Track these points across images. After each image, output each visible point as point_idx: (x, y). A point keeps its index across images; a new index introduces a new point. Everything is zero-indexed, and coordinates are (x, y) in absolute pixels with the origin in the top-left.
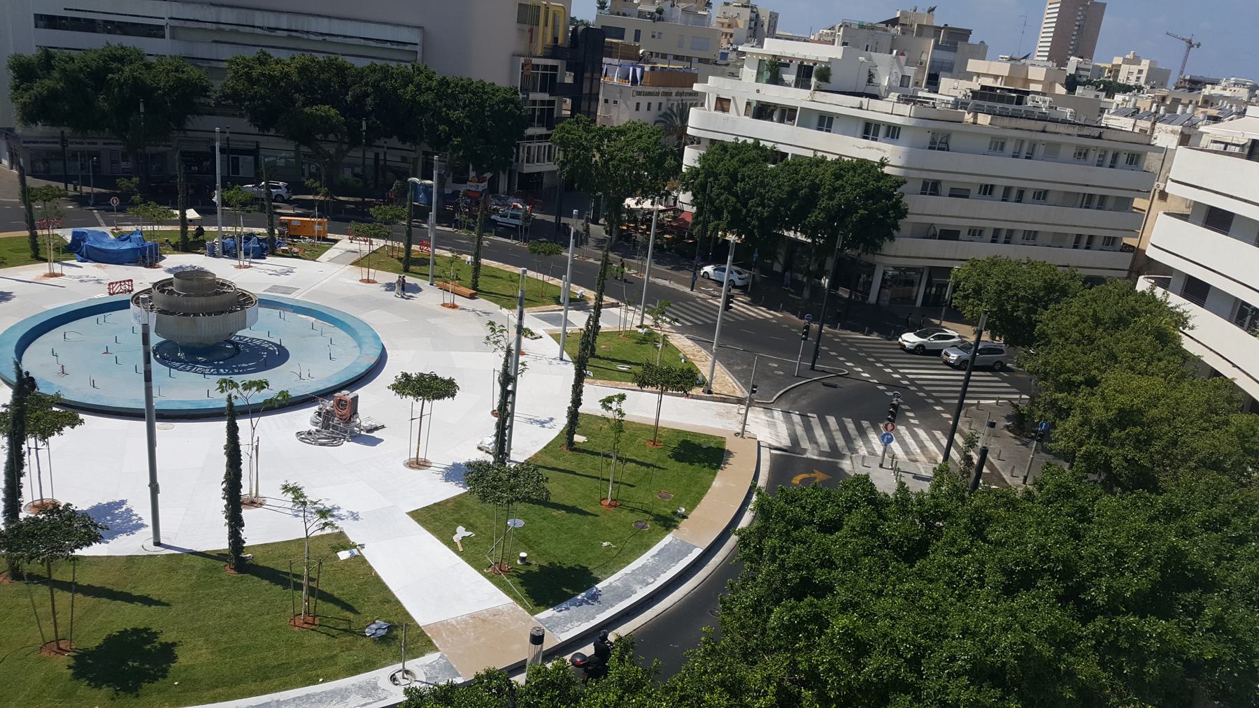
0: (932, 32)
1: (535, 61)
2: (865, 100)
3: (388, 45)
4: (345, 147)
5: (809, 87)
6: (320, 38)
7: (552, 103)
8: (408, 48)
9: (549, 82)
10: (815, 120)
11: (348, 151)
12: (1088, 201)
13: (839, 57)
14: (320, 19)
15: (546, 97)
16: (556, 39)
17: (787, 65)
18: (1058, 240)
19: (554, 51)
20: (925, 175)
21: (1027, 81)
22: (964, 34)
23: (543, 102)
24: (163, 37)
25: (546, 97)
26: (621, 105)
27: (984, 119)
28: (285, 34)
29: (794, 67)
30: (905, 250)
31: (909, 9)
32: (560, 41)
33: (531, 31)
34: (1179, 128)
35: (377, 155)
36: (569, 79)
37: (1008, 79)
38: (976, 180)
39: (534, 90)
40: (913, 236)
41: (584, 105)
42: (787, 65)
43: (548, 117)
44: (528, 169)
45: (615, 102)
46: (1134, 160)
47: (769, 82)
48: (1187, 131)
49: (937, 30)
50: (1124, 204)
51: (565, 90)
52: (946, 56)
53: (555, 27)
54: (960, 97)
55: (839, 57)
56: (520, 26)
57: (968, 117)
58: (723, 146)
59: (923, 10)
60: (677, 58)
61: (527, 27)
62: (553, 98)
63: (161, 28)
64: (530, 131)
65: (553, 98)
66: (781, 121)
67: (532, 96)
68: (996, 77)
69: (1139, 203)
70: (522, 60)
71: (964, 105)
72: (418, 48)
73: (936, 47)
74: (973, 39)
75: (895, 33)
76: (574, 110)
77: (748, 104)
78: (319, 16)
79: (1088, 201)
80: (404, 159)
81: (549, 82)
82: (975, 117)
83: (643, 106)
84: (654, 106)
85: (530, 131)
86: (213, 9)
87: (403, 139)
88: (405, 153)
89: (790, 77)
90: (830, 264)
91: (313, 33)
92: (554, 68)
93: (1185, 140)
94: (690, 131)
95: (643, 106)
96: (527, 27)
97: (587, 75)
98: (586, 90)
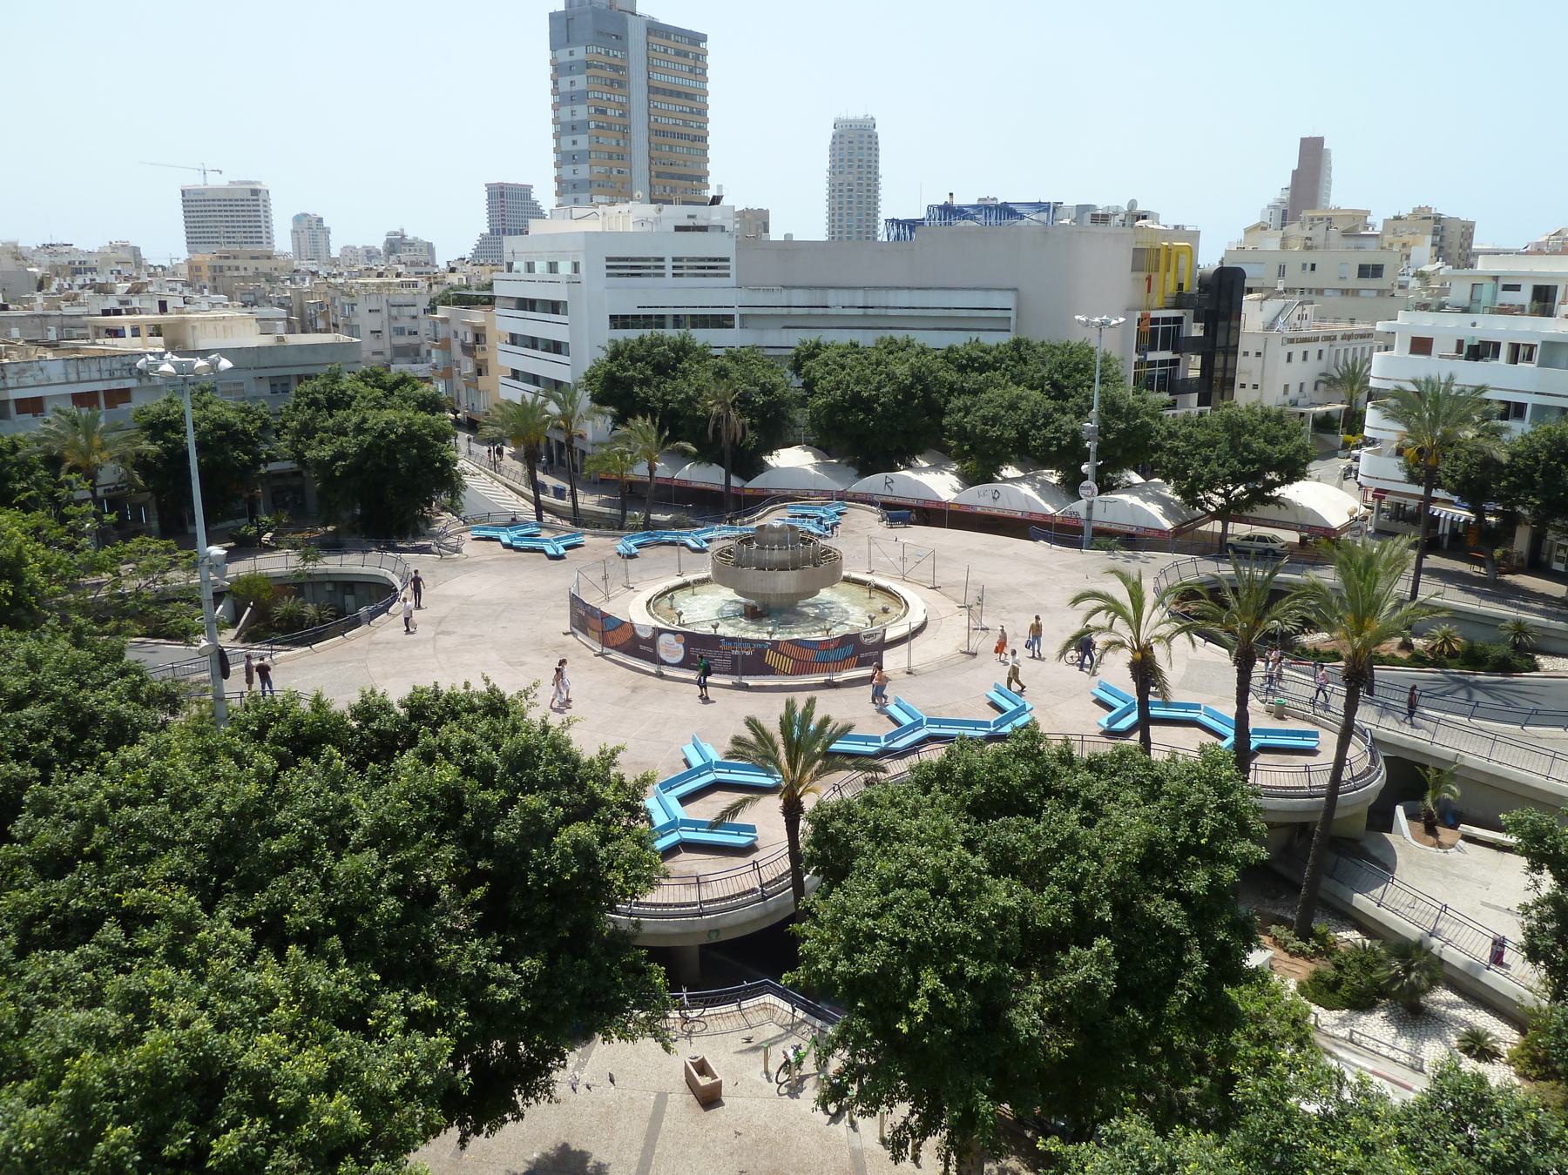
1: (1154, 314)
7: (1175, 362)
15: (1168, 355)
16: (1180, 286)
19: (1180, 300)
23: (1163, 363)
24: (732, 327)
25: (1168, 355)
32: (1185, 288)
33: (1149, 279)
36: (1197, 331)
39: (1153, 348)
41: (1219, 361)
45: (1258, 354)
51: (1194, 345)
56: (1135, 274)
62: (1177, 356)
63: (731, 317)
65: (1177, 356)
67: (1152, 356)
70: (1138, 315)
72: (1011, 314)
76: (1207, 368)
77: (1460, 343)
83: (1297, 356)
84: (1313, 355)
86: (785, 292)
92: (1178, 320)
94: (1373, 383)
95: (1297, 356)
96: (1144, 275)
97: (1222, 324)
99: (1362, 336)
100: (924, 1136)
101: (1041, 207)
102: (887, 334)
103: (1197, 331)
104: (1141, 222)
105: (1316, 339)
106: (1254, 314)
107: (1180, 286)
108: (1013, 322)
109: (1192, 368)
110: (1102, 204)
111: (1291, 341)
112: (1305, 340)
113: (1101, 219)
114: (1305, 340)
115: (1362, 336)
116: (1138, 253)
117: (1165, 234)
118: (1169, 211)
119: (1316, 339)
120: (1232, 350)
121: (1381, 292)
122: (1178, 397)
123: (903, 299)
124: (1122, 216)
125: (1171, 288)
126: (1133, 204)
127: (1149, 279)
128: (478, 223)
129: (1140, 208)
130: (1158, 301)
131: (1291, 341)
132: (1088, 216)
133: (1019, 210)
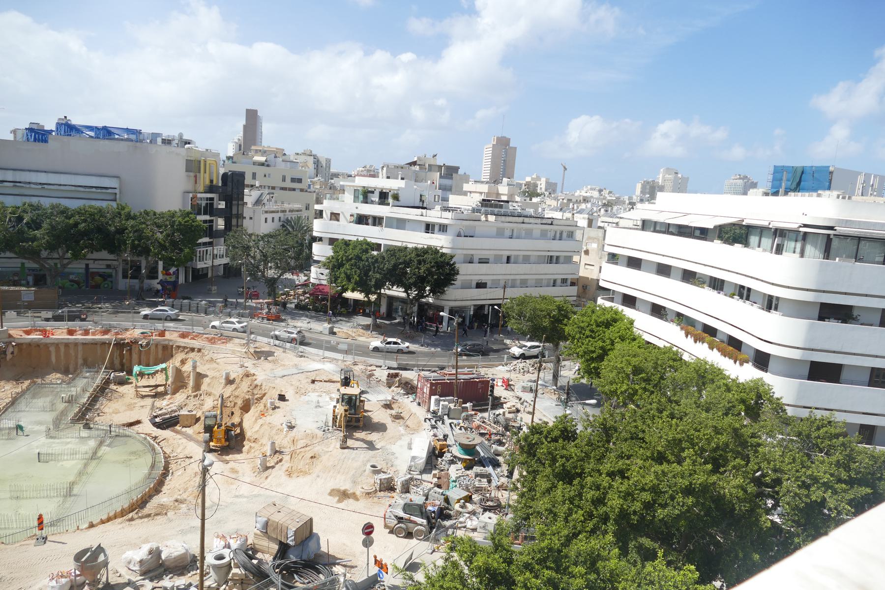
0: (437, 169)
1: (199, 195)
2: (424, 211)
3: (94, 190)
4: (65, 261)
5: (388, 204)
6: (40, 187)
7: (211, 221)
8: (110, 191)
9: (210, 209)
10: (395, 224)
11: (68, 264)
12: (551, 260)
13: (403, 186)
14: (39, 174)
15: (207, 217)
16: (211, 181)
17: (373, 192)
18: (539, 284)
19: (211, 189)
20: (465, 252)
21: (498, 194)
22: (455, 169)
23: (205, 222)
25: (207, 217)
26: (259, 220)
27: (491, 218)
28: (12, 184)
29: (377, 194)
30: (458, 295)
31: (421, 155)
32: (215, 182)
33: (196, 177)
34: (587, 216)
35: (87, 265)
36: (222, 205)
37: (488, 194)
38: (492, 252)
39: (200, 214)
40: (462, 288)
41: (234, 222)
42: (373, 192)
43: (210, 232)
44: (200, 265)
46: (571, 235)
47: (363, 202)
48: (591, 217)
49: (440, 167)
50: (568, 260)
52: (447, 182)
53: (211, 174)
54: (474, 206)
55: (403, 186)
57: (483, 218)
58: (347, 243)
59: (429, 155)
60: (294, 190)
61: (192, 174)
64: (200, 241)
66: (374, 225)
68: (481, 193)
69: (576, 258)
70: (191, 195)
71: (479, 211)
72: (117, 191)
73: (441, 177)
74: (460, 172)
75: (416, 168)
76: (228, 226)
78: (37, 171)
79: (551, 260)
80: (108, 266)
81: (210, 209)
82: (486, 217)
83: (269, 220)
85: (200, 241)
87: (111, 252)
88: (109, 263)
89: (376, 198)
90: (415, 309)
91: (34, 184)
92: (212, 199)
93: (590, 223)
95: (269, 220)
97: (234, 202)
98: (234, 211)
99: (297, 211)
100: (445, 526)
101: (127, 130)
102: (27, 200)
103: (222, 205)
104: (187, 146)
105: (278, 212)
106: (250, 197)
107: (211, 181)
108: (118, 196)
109: (220, 224)
110: (167, 133)
111: (266, 212)
112: (273, 212)
113: (167, 142)
114: (273, 212)
115: (297, 211)
116: (189, 162)
117: (202, 153)
118: (201, 144)
119: (278, 212)
120: (240, 216)
121: (302, 190)
122: (215, 241)
123: (42, 178)
124: (176, 141)
125: (208, 182)
126: (181, 135)
127: (196, 177)
128: (12, 135)
129: (185, 137)
130: (201, 189)
131: (266, 212)
132: (159, 140)
133: (113, 130)
